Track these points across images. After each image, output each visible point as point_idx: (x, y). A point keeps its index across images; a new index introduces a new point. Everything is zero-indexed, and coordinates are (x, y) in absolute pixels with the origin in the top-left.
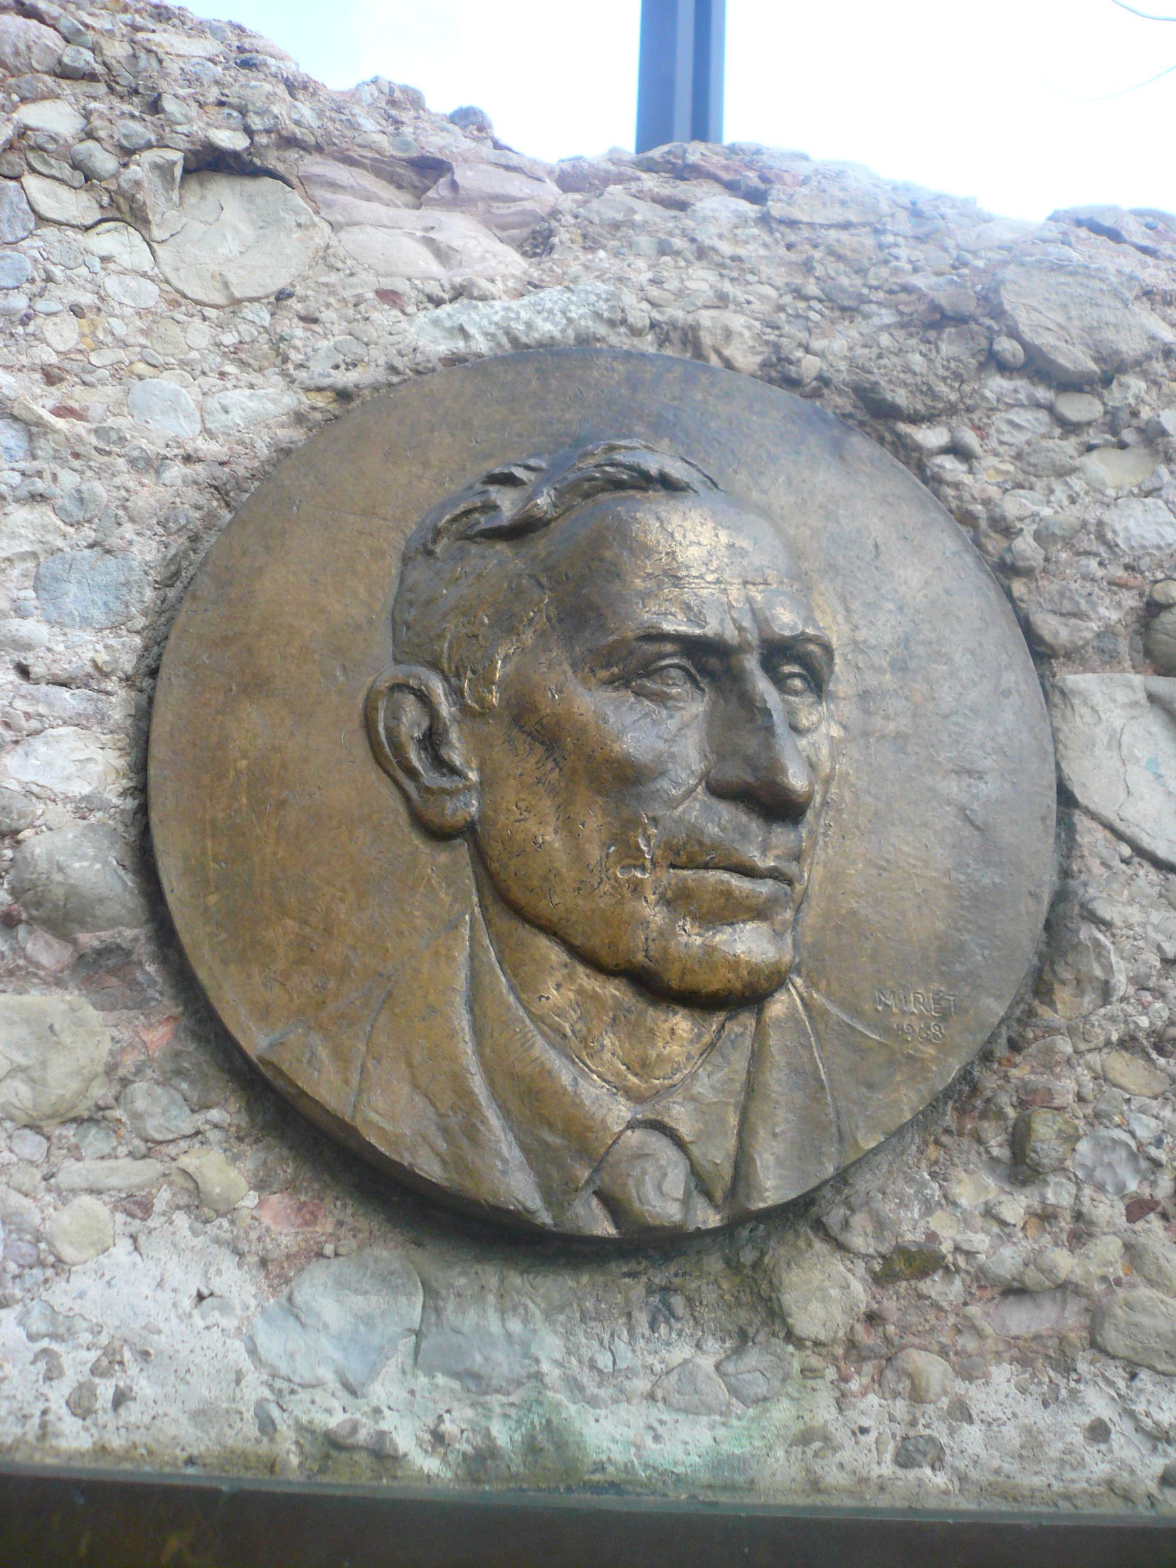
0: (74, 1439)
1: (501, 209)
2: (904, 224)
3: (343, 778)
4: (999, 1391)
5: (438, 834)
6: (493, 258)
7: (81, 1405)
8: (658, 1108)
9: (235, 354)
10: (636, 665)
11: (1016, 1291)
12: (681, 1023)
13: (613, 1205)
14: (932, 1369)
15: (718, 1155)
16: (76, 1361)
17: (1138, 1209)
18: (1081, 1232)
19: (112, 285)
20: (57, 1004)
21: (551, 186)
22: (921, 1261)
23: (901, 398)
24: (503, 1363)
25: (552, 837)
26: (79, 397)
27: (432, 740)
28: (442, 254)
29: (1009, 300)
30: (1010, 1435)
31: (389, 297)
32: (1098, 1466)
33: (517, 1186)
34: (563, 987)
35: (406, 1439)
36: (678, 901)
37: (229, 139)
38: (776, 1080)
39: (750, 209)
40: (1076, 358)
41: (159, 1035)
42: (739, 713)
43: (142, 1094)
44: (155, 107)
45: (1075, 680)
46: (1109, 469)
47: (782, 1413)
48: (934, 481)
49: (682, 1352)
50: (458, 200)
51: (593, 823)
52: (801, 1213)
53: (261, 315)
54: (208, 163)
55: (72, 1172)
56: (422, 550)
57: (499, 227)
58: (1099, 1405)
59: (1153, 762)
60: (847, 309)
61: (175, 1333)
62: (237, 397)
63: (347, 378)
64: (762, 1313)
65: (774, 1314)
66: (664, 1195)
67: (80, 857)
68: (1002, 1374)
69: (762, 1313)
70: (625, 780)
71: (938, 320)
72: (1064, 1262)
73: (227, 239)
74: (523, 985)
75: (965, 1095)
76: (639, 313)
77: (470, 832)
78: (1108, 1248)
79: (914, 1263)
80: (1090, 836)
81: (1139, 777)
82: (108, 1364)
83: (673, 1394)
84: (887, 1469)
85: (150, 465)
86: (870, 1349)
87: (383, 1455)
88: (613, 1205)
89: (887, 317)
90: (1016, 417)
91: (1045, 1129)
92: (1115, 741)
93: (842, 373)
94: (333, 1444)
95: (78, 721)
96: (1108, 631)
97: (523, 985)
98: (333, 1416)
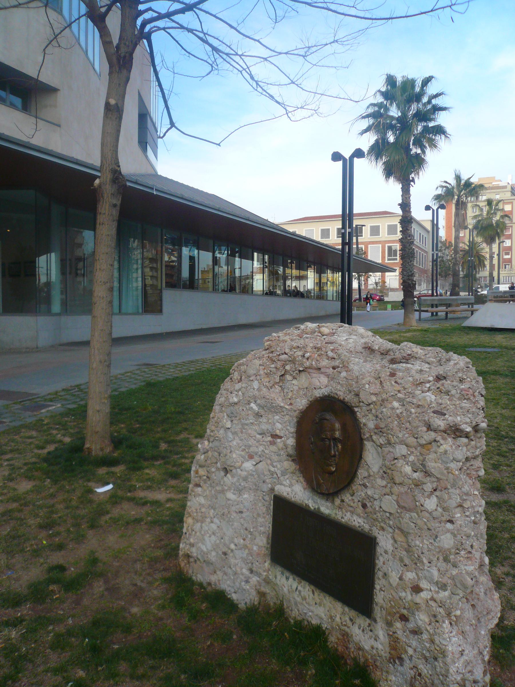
0: (293, 499)
1: (326, 374)
14: (344, 511)
17: (359, 501)
19: (294, 387)
21: (331, 369)
26: (293, 401)
31: (315, 388)
32: (354, 523)
35: (310, 506)
37: (301, 369)
45: (365, 442)
47: (334, 511)
49: (328, 504)
50: (322, 373)
53: (305, 390)
54: (300, 371)
55: (294, 478)
59: (372, 453)
67: (291, 451)
68: (349, 513)
72: (352, 504)
73: (303, 380)
78: (356, 504)
80: (363, 461)
81: (370, 455)
82: (295, 494)
83: (327, 508)
84: (340, 518)
85: (295, 411)
86: (340, 508)
89: (353, 393)
92: (369, 450)
94: (306, 504)
95: (292, 437)
96: (367, 438)
98: (307, 502)
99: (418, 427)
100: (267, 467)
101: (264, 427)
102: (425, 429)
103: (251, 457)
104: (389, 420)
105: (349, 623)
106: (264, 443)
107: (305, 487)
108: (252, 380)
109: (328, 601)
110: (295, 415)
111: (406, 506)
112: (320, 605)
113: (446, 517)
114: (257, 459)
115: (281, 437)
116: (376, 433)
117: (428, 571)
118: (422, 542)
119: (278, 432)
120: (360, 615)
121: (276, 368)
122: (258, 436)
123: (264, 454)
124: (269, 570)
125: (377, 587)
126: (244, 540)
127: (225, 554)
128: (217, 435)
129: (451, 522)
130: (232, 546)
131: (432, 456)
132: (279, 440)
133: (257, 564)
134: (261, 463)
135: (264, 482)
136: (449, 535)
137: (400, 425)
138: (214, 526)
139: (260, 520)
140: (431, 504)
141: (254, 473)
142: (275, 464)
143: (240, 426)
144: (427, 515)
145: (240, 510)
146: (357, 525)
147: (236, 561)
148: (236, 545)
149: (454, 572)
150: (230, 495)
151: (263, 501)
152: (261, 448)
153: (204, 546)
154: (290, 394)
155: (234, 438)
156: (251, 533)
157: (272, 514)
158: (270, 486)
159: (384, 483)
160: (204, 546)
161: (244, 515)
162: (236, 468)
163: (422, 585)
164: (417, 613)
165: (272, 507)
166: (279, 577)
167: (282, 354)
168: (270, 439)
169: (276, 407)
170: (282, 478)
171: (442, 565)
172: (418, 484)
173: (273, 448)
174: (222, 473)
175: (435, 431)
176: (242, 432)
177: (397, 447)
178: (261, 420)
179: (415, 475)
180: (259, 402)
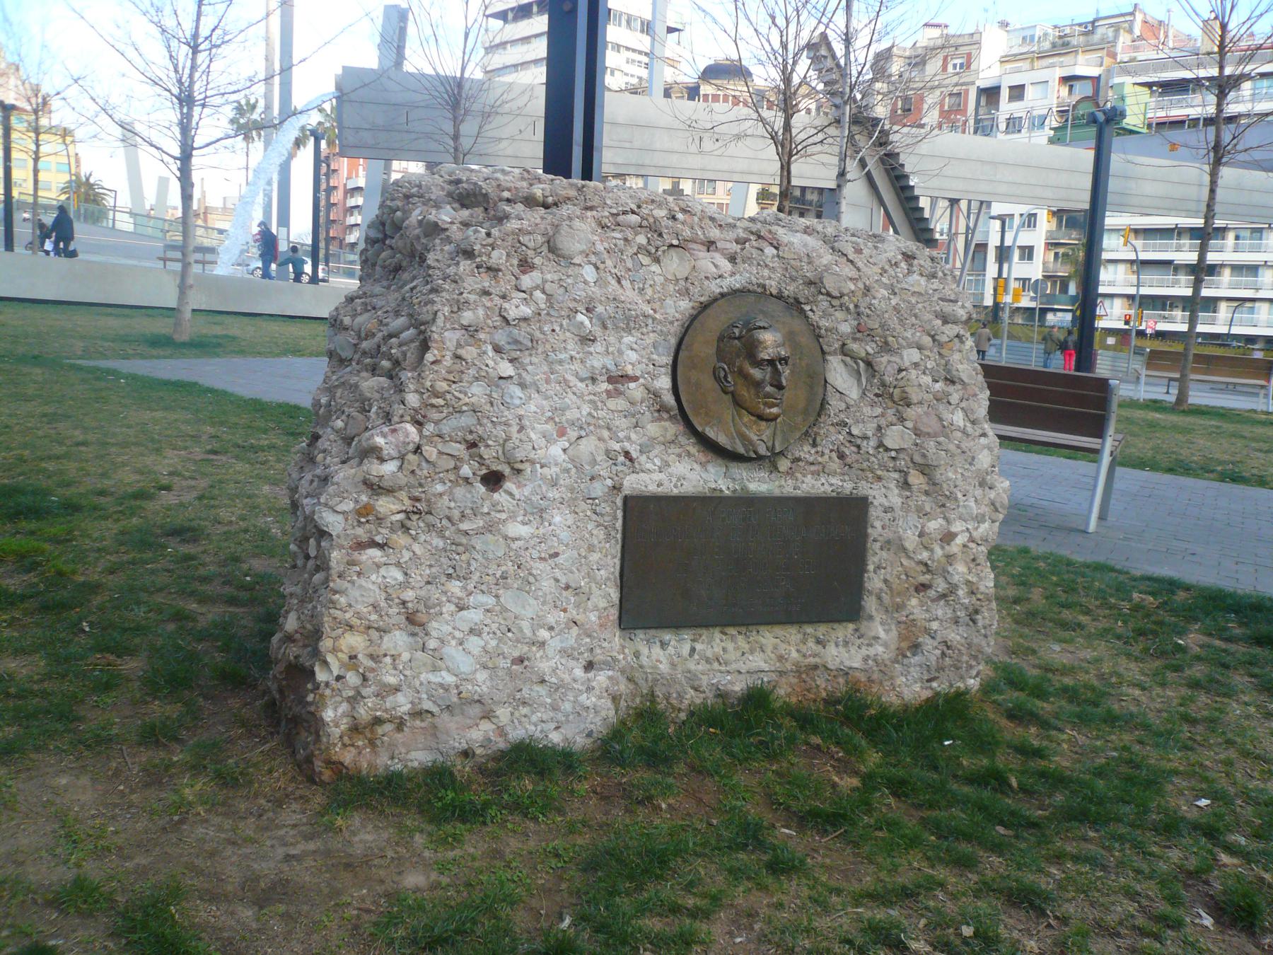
0: (676, 491)
2: (805, 259)
3: (709, 383)
4: (809, 479)
5: (726, 393)
6: (726, 265)
7: (676, 486)
8: (760, 437)
9: (678, 292)
10: (758, 364)
11: (812, 464)
12: (764, 423)
13: (756, 452)
14: (799, 475)
15: (770, 444)
16: (674, 480)
18: (823, 454)
20: (667, 424)
22: (799, 459)
23: (802, 300)
24: (738, 477)
25: (745, 394)
27: (726, 377)
28: (716, 266)
29: (825, 281)
30: (810, 485)
31: (707, 278)
33: (741, 450)
34: (747, 418)
36: (766, 404)
37: (675, 242)
38: (778, 432)
39: (775, 252)
40: (836, 293)
41: (681, 428)
42: (777, 373)
43: (680, 438)
44: (660, 235)
45: (829, 358)
46: (840, 315)
48: (807, 317)
51: (752, 391)
52: (782, 453)
54: (672, 246)
56: (721, 339)
57: (723, 254)
58: (823, 481)
60: (793, 279)
61: (689, 475)
62: (681, 303)
63: (702, 299)
64: (774, 468)
65: (776, 468)
66: (762, 450)
69: (774, 468)
70: (758, 385)
71: (811, 283)
72: (820, 459)
73: (674, 264)
74: (741, 418)
75: (806, 434)
76: (754, 280)
77: (733, 393)
79: (797, 460)
82: (679, 480)
85: (672, 323)
86: (790, 473)
87: (721, 491)
88: (756, 452)
90: (824, 302)
91: (818, 439)
93: (792, 295)
97: (741, 418)
99: (930, 321)
100: (602, 445)
101: (597, 363)
102: (939, 322)
103: (562, 433)
104: (886, 316)
105: (818, 648)
106: (592, 397)
107: (703, 460)
108: (580, 265)
109: (768, 637)
110: (672, 331)
111: (930, 430)
112: (752, 651)
113: (979, 432)
114: (573, 434)
115: (635, 379)
116: (855, 339)
117: (965, 506)
118: (956, 472)
119: (629, 370)
120: (836, 626)
121: (626, 240)
122: (581, 385)
123: (593, 421)
124: (624, 647)
125: (871, 567)
126: (565, 611)
127: (521, 660)
128: (467, 400)
129: (984, 435)
130: (544, 634)
131: (957, 356)
132: (632, 385)
133: (605, 644)
134: (584, 441)
135: (592, 479)
136: (986, 452)
137: (901, 321)
138: (474, 616)
139: (595, 557)
140: (958, 418)
141: (570, 466)
142: (621, 435)
143: (546, 368)
144: (959, 434)
145: (552, 552)
146: (828, 489)
147: (552, 663)
148: (551, 628)
149: (992, 495)
150: (516, 529)
151: (594, 517)
152: (586, 409)
153: (444, 673)
154: (649, 292)
155: (530, 398)
156: (577, 591)
157: (619, 536)
158: (609, 482)
159: (879, 411)
160: (444, 673)
161: (560, 560)
162: (533, 462)
163: (953, 529)
164: (950, 569)
165: (619, 524)
166: (645, 651)
167: (625, 213)
168: (605, 386)
169: (637, 316)
170: (643, 458)
171: (978, 492)
172: (942, 398)
173: (619, 404)
174: (482, 489)
175: (954, 323)
176: (548, 381)
177: (905, 353)
178: (592, 349)
179: (939, 386)
180: (600, 309)
